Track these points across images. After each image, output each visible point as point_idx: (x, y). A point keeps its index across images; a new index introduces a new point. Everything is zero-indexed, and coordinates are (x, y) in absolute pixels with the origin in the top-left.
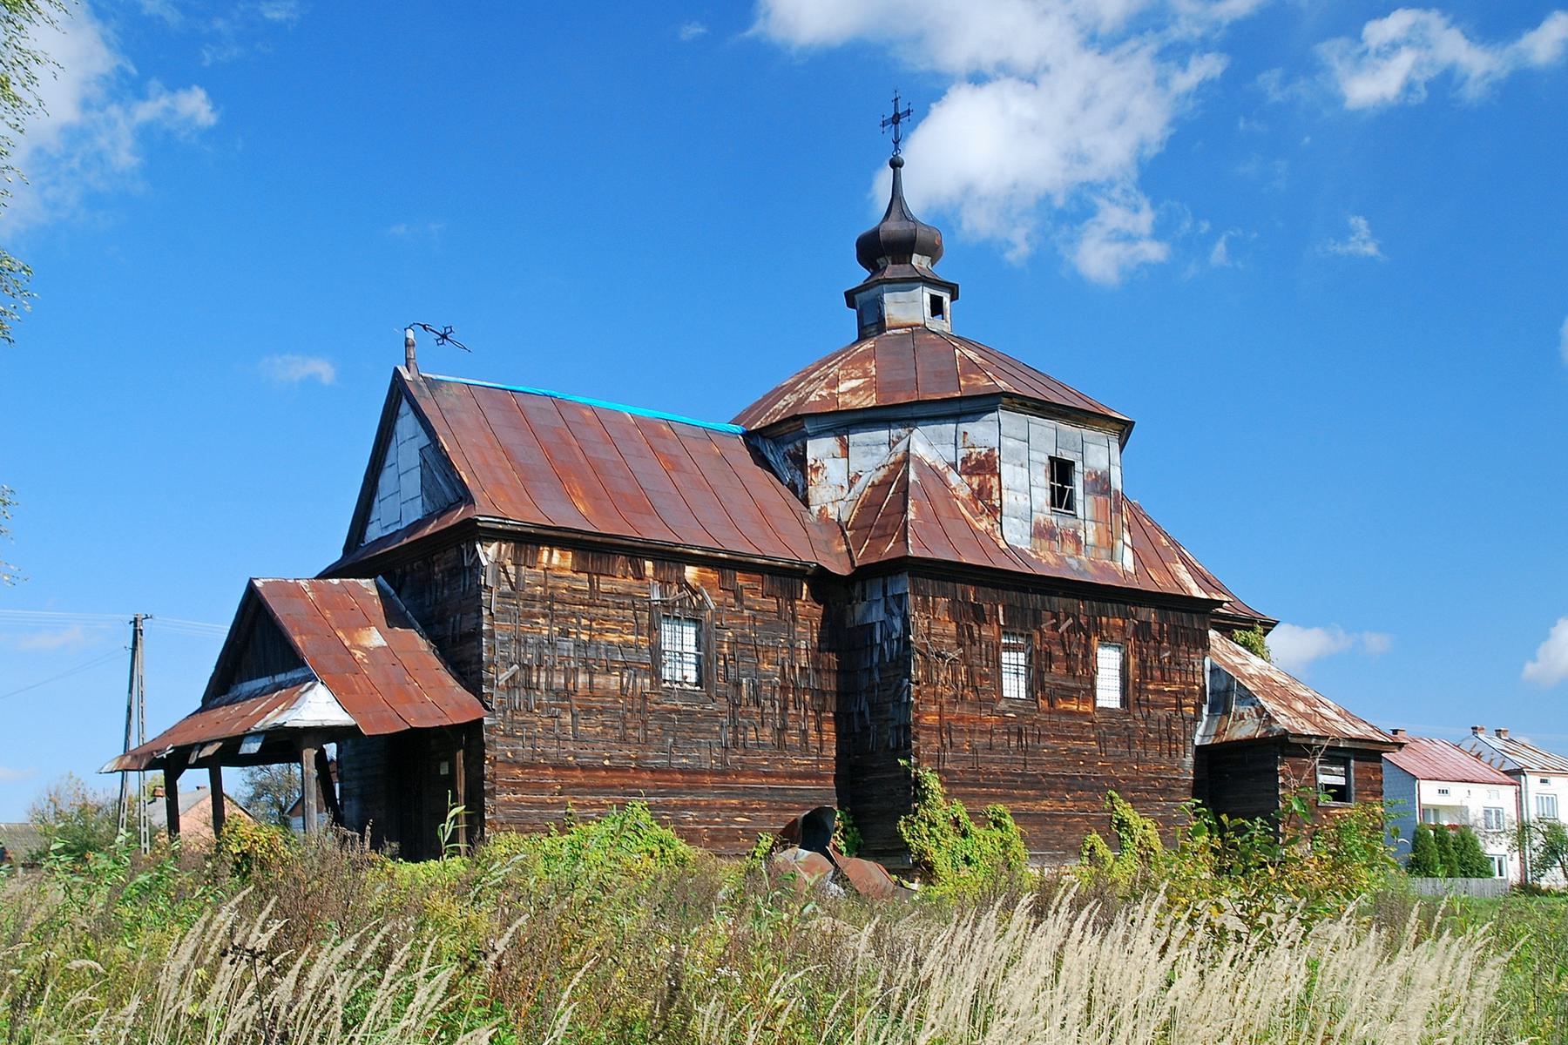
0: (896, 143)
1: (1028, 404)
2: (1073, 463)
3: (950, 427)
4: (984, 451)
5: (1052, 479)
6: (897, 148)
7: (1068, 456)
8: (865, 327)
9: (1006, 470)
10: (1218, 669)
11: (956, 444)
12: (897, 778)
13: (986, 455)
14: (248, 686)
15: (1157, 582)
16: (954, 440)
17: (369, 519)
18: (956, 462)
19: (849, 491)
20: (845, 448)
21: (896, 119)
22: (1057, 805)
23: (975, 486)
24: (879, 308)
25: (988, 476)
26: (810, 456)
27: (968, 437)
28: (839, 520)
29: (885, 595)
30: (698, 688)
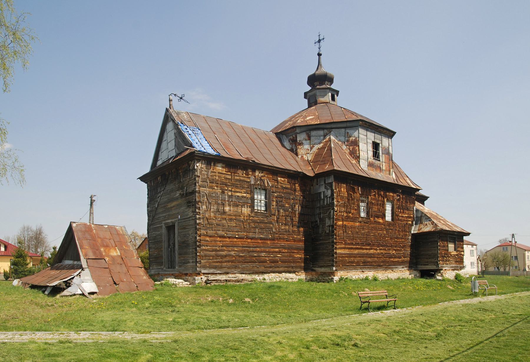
1: (367, 124)
2: (379, 144)
4: (354, 138)
5: (373, 149)
7: (378, 141)
8: (310, 103)
9: (361, 144)
10: (418, 210)
12: (329, 242)
15: (402, 182)
21: (319, 41)
22: (375, 251)
23: (351, 149)
24: (315, 97)
26: (298, 140)
28: (308, 160)
29: (325, 182)
30: (266, 212)
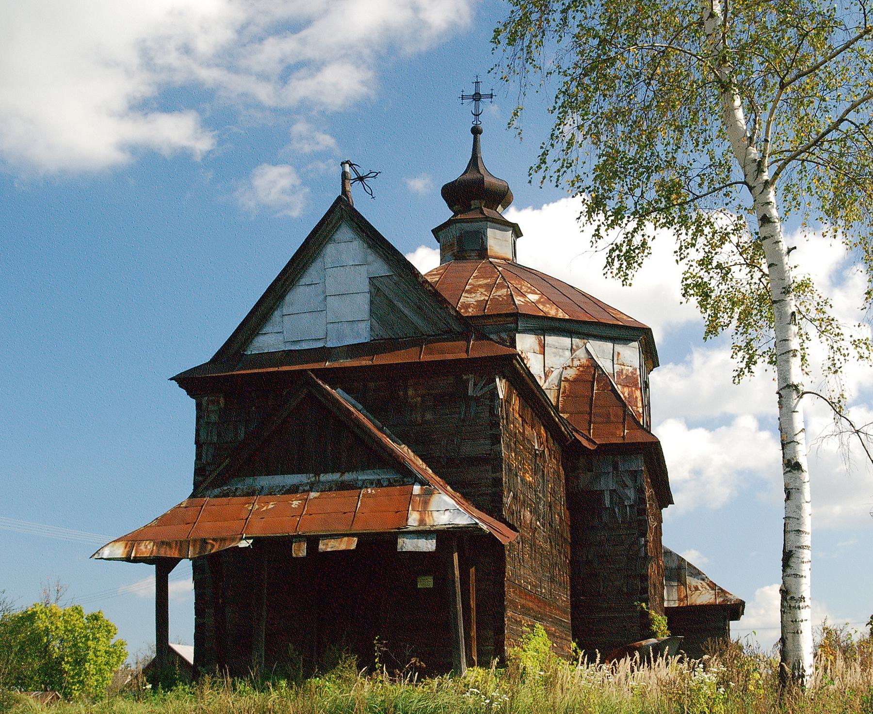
0: (477, 115)
3: (609, 345)
4: (630, 369)
6: (477, 120)
11: (613, 360)
13: (632, 373)
14: (264, 481)
16: (611, 356)
17: (261, 328)
18: (614, 373)
19: (545, 382)
20: (543, 347)
21: (477, 97)
24: (482, 239)
25: (633, 389)
27: (621, 356)
29: (616, 468)
